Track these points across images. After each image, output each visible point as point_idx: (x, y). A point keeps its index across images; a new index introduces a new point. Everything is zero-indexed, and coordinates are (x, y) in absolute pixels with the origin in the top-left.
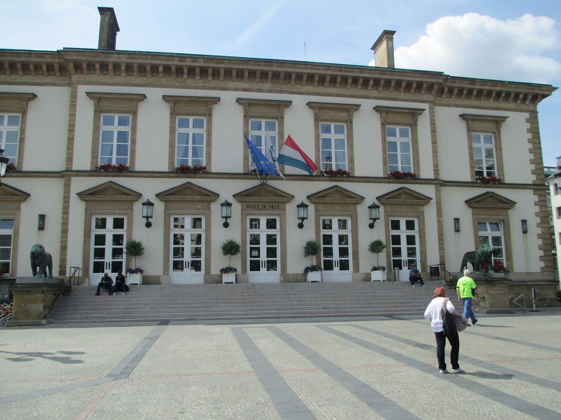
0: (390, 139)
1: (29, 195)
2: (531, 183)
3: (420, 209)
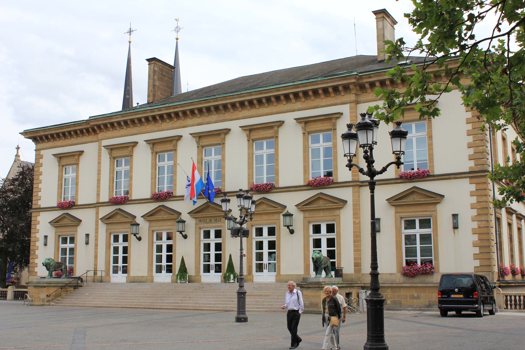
3: (337, 212)
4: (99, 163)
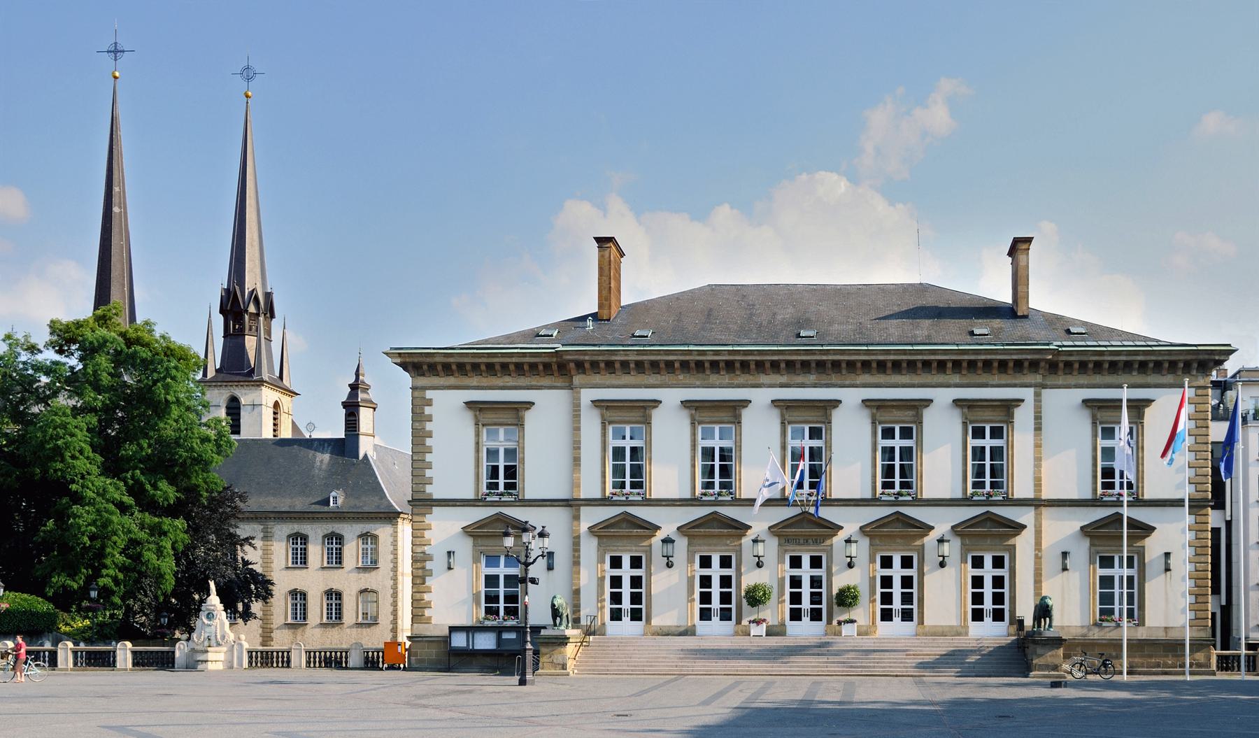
4: (577, 429)
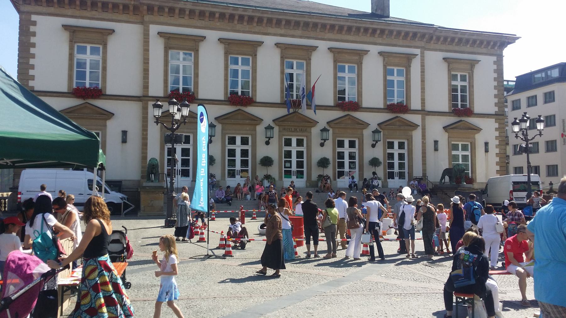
0: (389, 78)
1: (113, 114)
2: (494, 113)
